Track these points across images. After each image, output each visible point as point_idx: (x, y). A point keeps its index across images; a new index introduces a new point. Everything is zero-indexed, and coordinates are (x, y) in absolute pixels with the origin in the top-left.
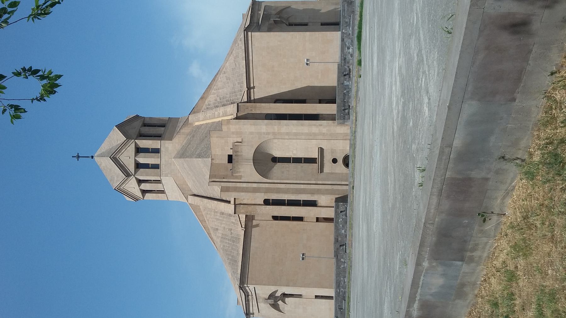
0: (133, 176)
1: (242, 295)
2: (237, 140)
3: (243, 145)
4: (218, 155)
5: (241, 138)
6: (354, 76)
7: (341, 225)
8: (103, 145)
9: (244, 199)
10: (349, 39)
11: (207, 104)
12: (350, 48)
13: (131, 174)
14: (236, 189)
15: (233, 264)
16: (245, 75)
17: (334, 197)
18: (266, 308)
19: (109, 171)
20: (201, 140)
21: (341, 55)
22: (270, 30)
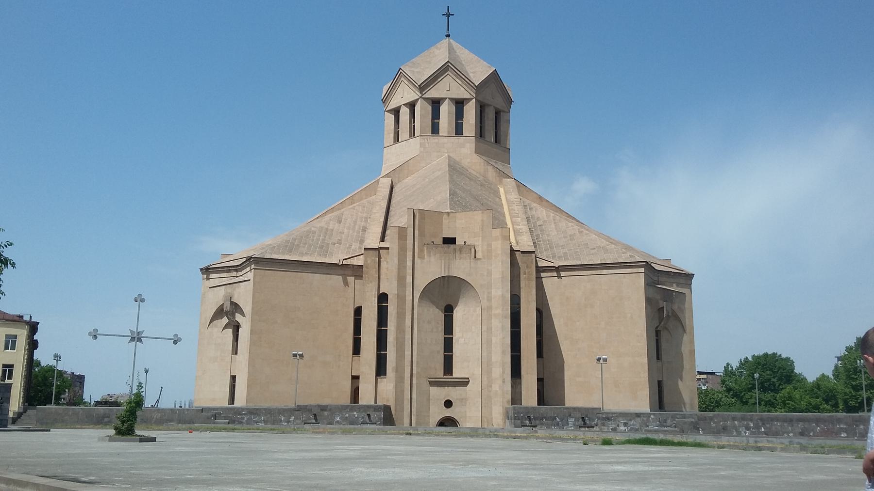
0: (420, 95)
1: (238, 262)
2: (478, 251)
3: (472, 261)
4: (456, 222)
6: (584, 433)
7: (347, 415)
8: (467, 51)
9: (387, 262)
10: (640, 426)
11: (532, 206)
12: (626, 428)
13: (423, 93)
14: (402, 250)
15: (286, 246)
16: (579, 263)
17: (391, 403)
18: (217, 298)
19: (428, 60)
20: (477, 197)
21: (615, 413)
22: (649, 301)
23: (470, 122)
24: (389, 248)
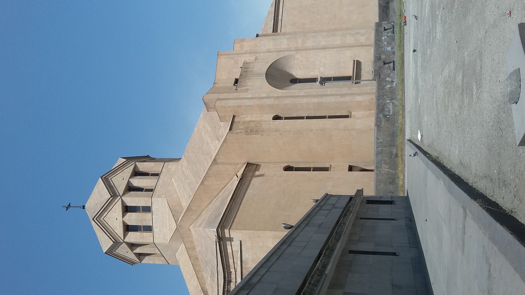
1: (220, 286)
5: (255, 56)
7: (385, 43)
9: (246, 117)
13: (118, 195)
23: (153, 166)
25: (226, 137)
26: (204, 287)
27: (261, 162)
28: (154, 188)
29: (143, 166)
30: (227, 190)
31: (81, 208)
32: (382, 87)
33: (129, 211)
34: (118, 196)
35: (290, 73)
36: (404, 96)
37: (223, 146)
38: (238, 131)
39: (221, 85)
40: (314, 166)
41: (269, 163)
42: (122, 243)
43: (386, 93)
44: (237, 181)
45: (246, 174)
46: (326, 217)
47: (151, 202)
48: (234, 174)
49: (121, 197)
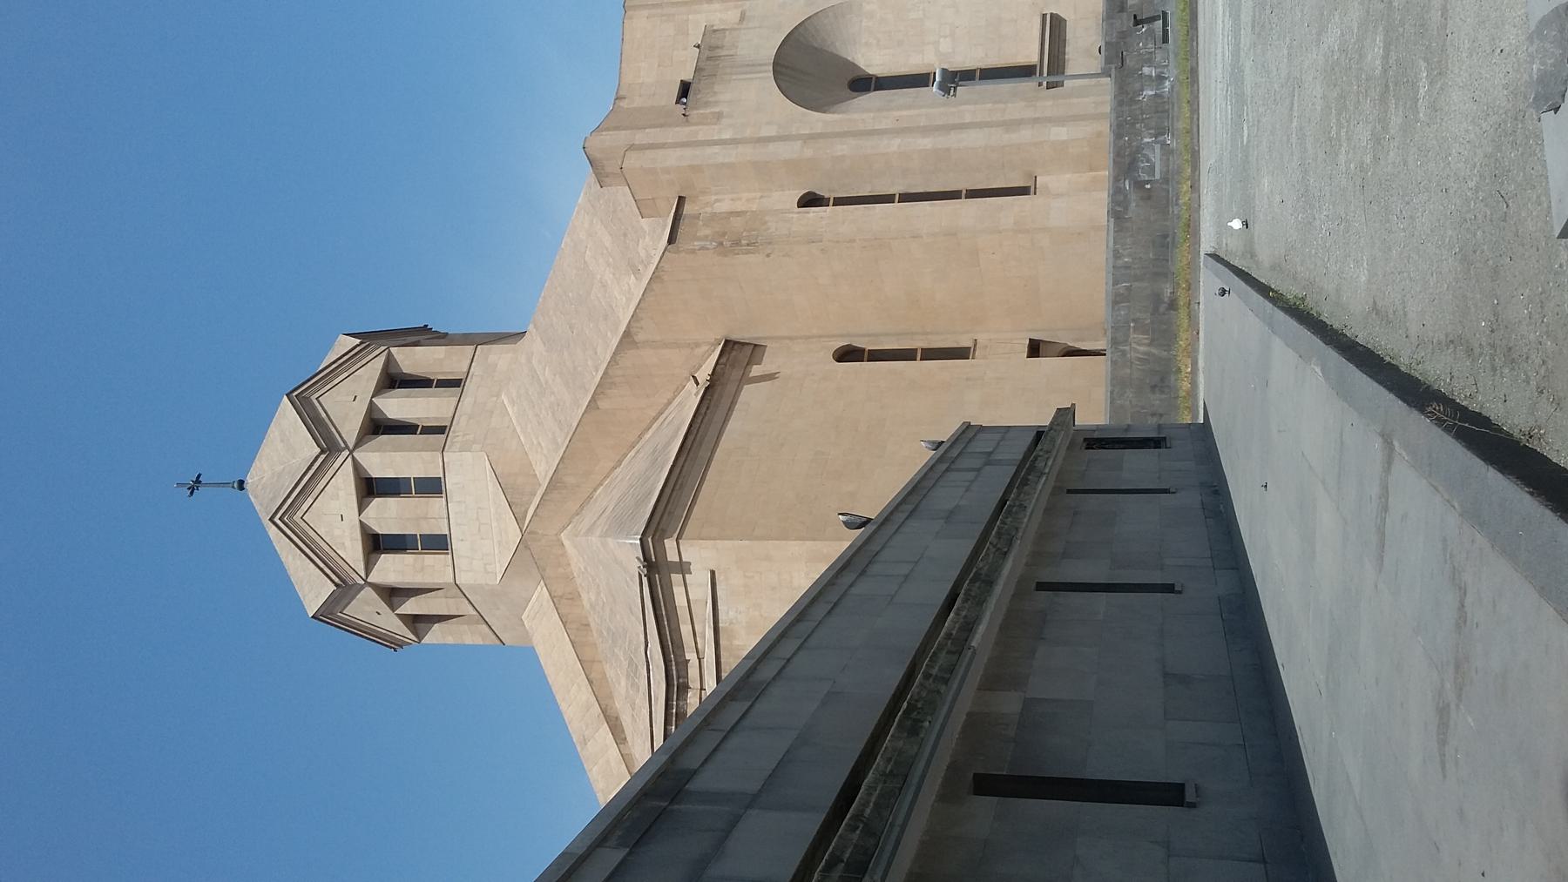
1: (657, 699)
5: (740, 10)
9: (717, 201)
13: (343, 445)
24: (680, 198)
25: (659, 262)
26: (609, 707)
27: (765, 338)
28: (448, 424)
29: (411, 359)
30: (666, 422)
31: (233, 487)
32: (1129, 97)
33: (378, 494)
34: (341, 450)
35: (849, 59)
36: (1195, 119)
37: (653, 290)
38: (696, 243)
39: (638, 102)
40: (926, 346)
41: (790, 338)
42: (362, 587)
43: (1142, 114)
44: (696, 395)
45: (724, 373)
46: (967, 491)
47: (441, 464)
48: (686, 374)
49: (351, 452)
